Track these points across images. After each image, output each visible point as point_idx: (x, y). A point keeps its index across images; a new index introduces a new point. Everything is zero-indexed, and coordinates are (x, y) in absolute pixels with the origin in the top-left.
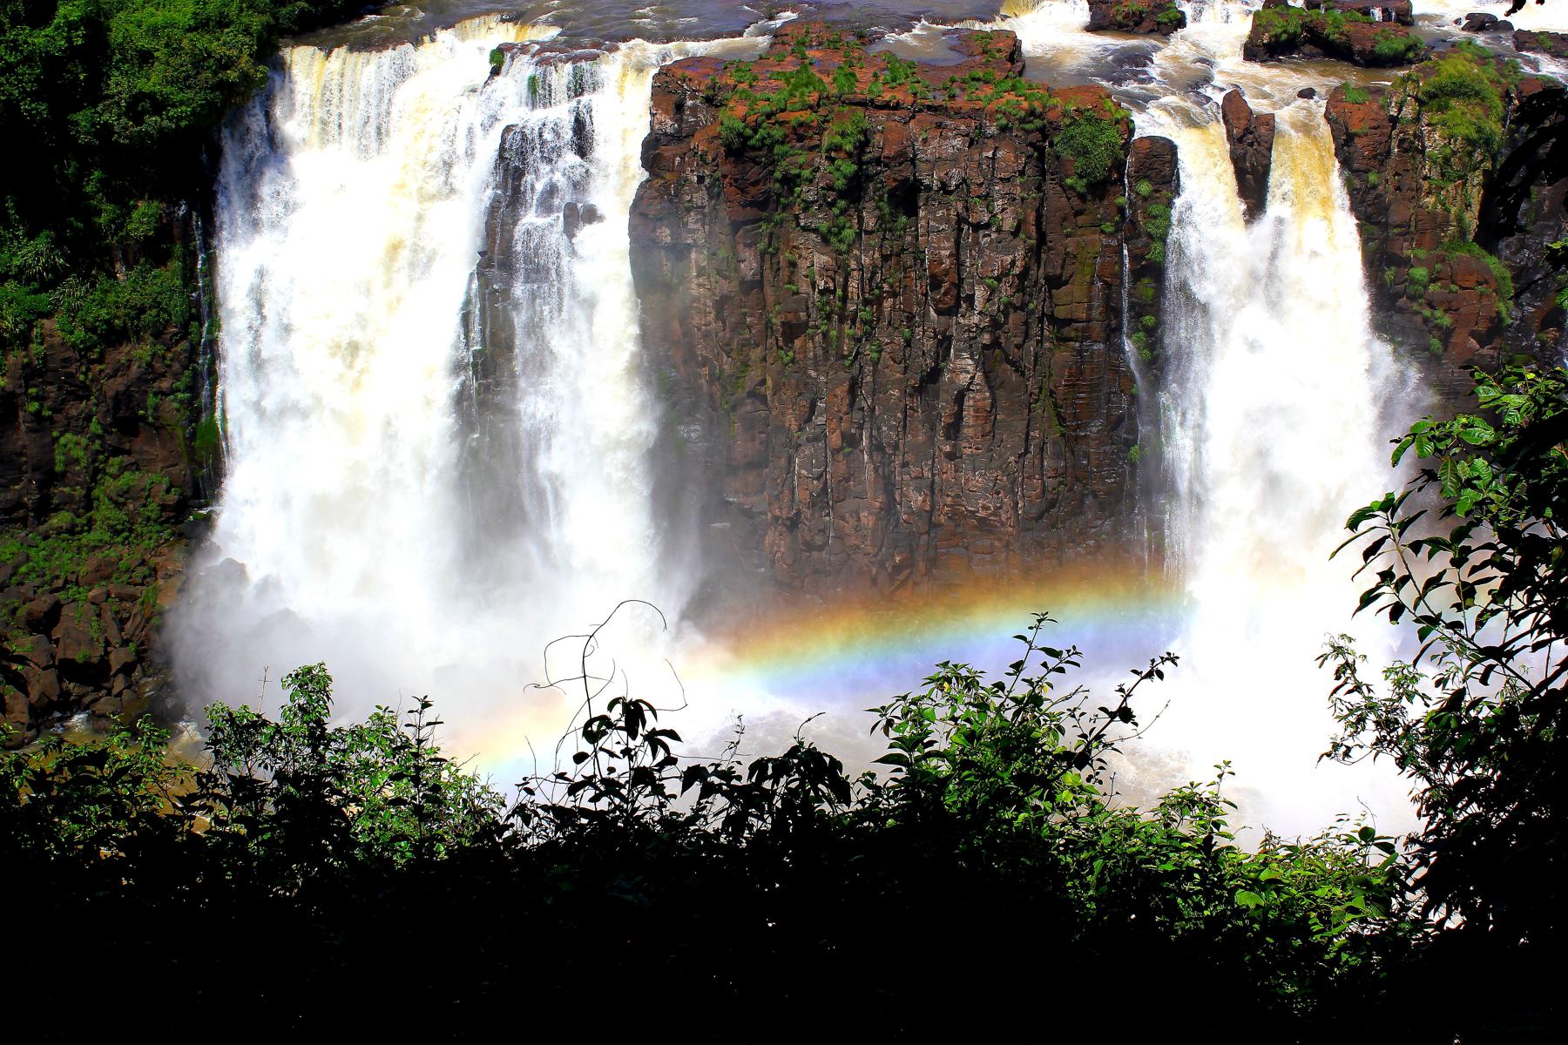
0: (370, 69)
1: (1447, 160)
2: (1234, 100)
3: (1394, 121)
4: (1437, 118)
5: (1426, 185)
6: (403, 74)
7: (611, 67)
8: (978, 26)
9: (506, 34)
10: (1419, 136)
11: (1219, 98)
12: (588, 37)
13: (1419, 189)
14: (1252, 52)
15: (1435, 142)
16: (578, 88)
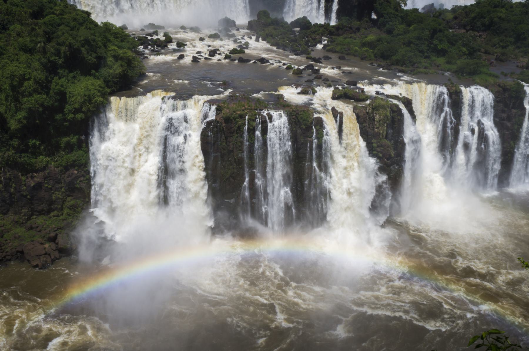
0: (131, 101)
1: (379, 121)
2: (333, 109)
3: (367, 113)
4: (377, 112)
5: (375, 127)
6: (138, 104)
7: (191, 102)
8: (274, 93)
9: (163, 94)
10: (373, 116)
11: (330, 108)
12: (183, 95)
13: (374, 128)
14: (334, 98)
15: (377, 118)
16: (185, 107)
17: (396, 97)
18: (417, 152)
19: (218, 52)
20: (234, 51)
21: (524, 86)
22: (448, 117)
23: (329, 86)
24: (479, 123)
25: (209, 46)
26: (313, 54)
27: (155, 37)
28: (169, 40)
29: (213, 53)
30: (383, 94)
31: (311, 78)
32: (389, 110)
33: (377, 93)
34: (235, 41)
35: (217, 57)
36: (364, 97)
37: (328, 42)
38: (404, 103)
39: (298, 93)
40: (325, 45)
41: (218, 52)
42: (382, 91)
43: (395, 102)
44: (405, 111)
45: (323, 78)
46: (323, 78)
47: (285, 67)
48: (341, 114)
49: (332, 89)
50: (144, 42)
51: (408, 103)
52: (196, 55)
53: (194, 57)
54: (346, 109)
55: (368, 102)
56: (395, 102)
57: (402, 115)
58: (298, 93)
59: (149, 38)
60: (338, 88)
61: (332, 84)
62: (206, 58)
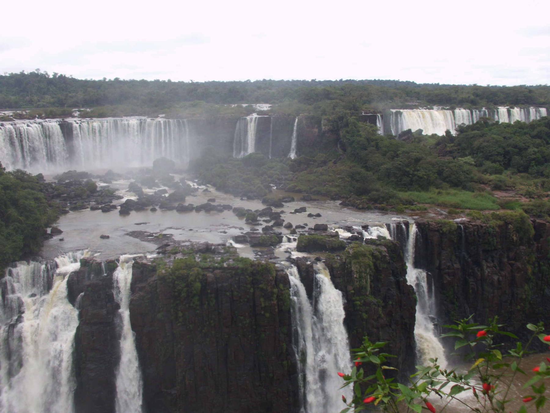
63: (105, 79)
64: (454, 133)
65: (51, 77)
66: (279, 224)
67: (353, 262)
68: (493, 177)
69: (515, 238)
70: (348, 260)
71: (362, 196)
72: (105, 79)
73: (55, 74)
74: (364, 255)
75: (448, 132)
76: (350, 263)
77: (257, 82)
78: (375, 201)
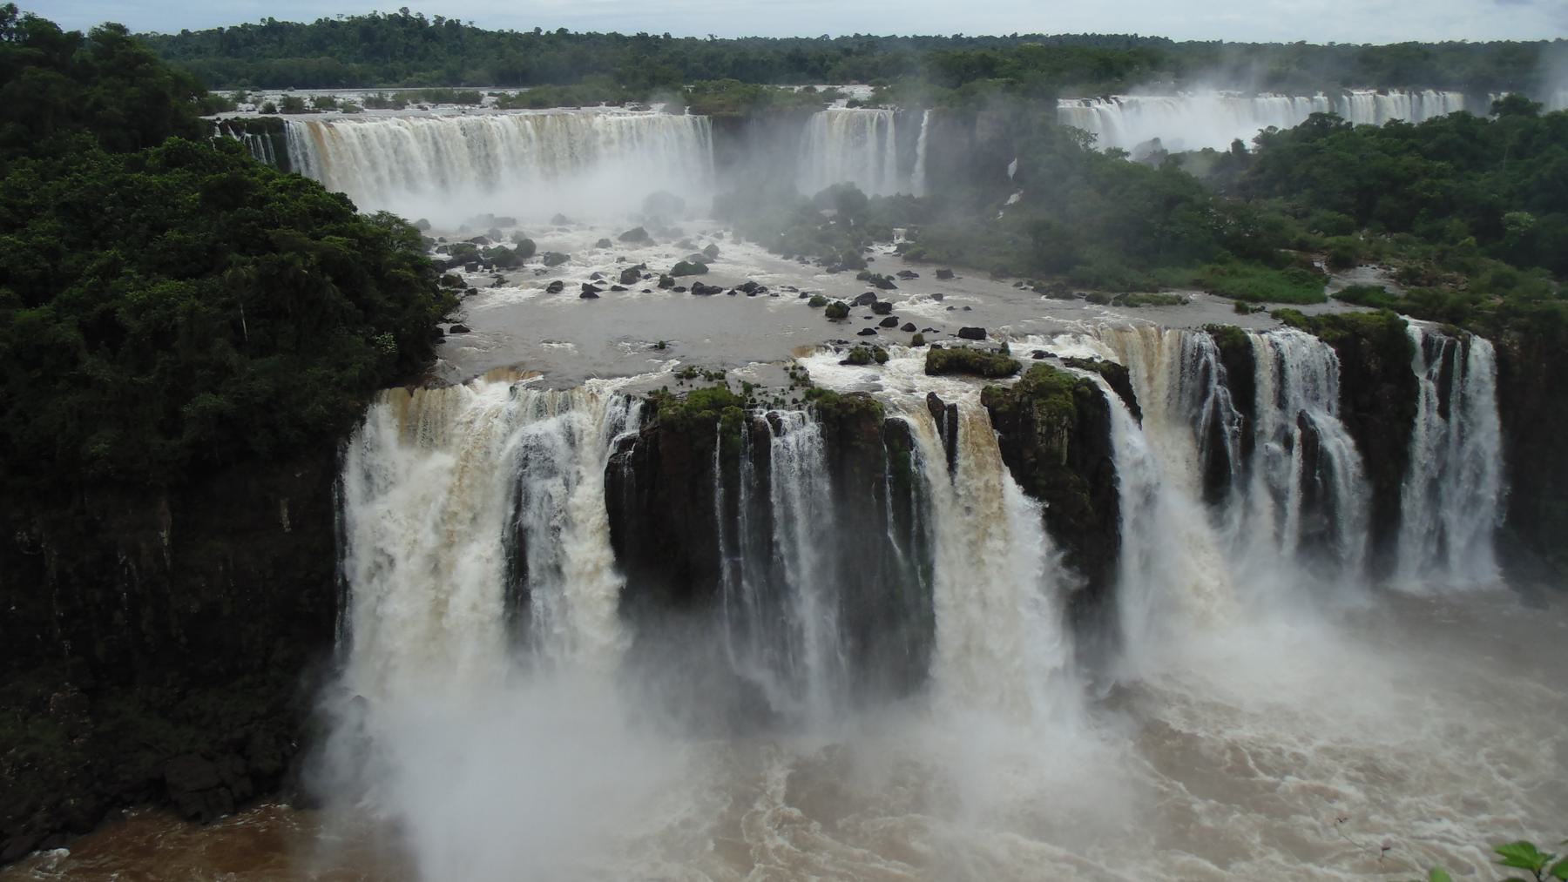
4: (1041, 401)
11: (924, 396)
17: (1088, 364)
18: (1148, 498)
19: (643, 273)
20: (681, 269)
21: (1406, 324)
22: (1223, 408)
23: (918, 342)
24: (1303, 420)
25: (622, 259)
26: (872, 269)
27: (493, 245)
28: (526, 249)
29: (631, 276)
30: (1053, 356)
31: (872, 324)
32: (1070, 394)
33: (1039, 355)
34: (685, 245)
35: (642, 285)
36: (1003, 366)
37: (908, 236)
38: (1106, 376)
39: (843, 363)
40: (901, 248)
41: (643, 273)
42: (1048, 349)
43: (1082, 374)
44: (1111, 395)
45: (902, 323)
46: (902, 323)
47: (808, 300)
48: (953, 408)
49: (925, 349)
50: (466, 255)
51: (1118, 377)
52: (589, 282)
53: (585, 286)
54: (963, 394)
55: (1017, 378)
56: (1082, 374)
57: (1104, 405)
58: (843, 363)
59: (480, 247)
60: (939, 347)
61: (926, 336)
62: (615, 289)
63: (538, 30)
64: (1250, 145)
65: (431, 24)
66: (890, 323)
67: (1034, 402)
68: (1331, 240)
69: (1373, 367)
70: (1025, 399)
71: (1060, 270)
72: (538, 30)
73: (439, 19)
74: (1060, 391)
75: (1238, 145)
76: (1030, 404)
77: (844, 39)
78: (1082, 284)
